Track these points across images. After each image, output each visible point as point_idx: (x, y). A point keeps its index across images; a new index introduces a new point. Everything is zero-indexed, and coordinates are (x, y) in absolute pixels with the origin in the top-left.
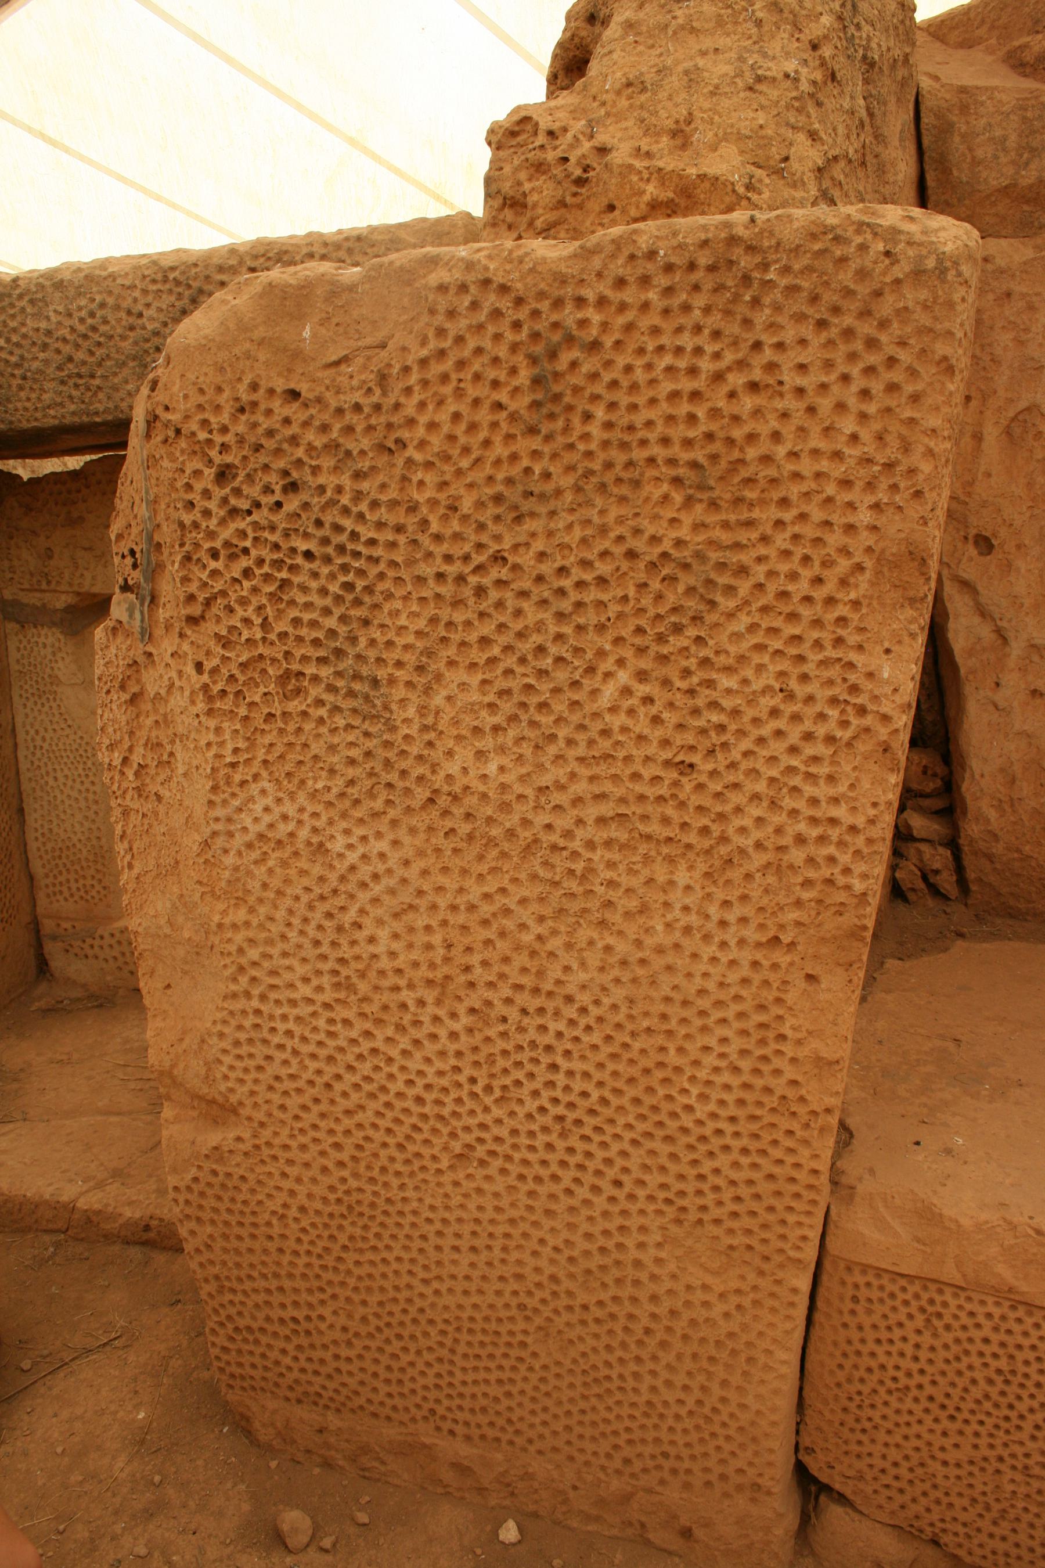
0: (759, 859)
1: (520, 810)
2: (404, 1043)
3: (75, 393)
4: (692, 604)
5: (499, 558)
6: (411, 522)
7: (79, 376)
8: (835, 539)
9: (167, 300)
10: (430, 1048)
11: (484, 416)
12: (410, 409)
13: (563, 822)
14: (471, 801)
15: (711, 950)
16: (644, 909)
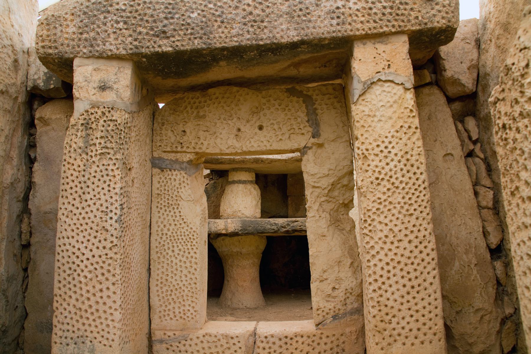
3: (251, 29)
7: (255, 21)
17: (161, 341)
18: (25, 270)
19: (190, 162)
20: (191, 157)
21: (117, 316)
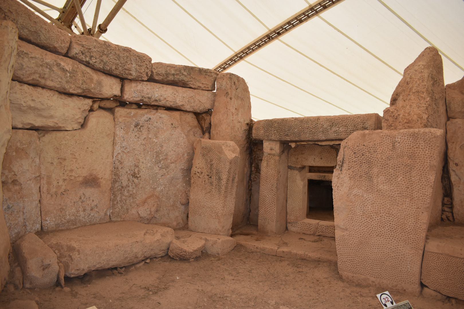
0: (416, 199)
1: (388, 192)
2: (371, 220)
4: (409, 170)
5: (387, 164)
6: (377, 160)
8: (425, 164)
9: (328, 124)
10: (374, 221)
11: (386, 149)
12: (378, 147)
13: (393, 194)
14: (382, 191)
15: (410, 209)
16: (402, 204)
17: (290, 223)
18: (250, 197)
19: (300, 168)
20: (300, 166)
21: (275, 214)
